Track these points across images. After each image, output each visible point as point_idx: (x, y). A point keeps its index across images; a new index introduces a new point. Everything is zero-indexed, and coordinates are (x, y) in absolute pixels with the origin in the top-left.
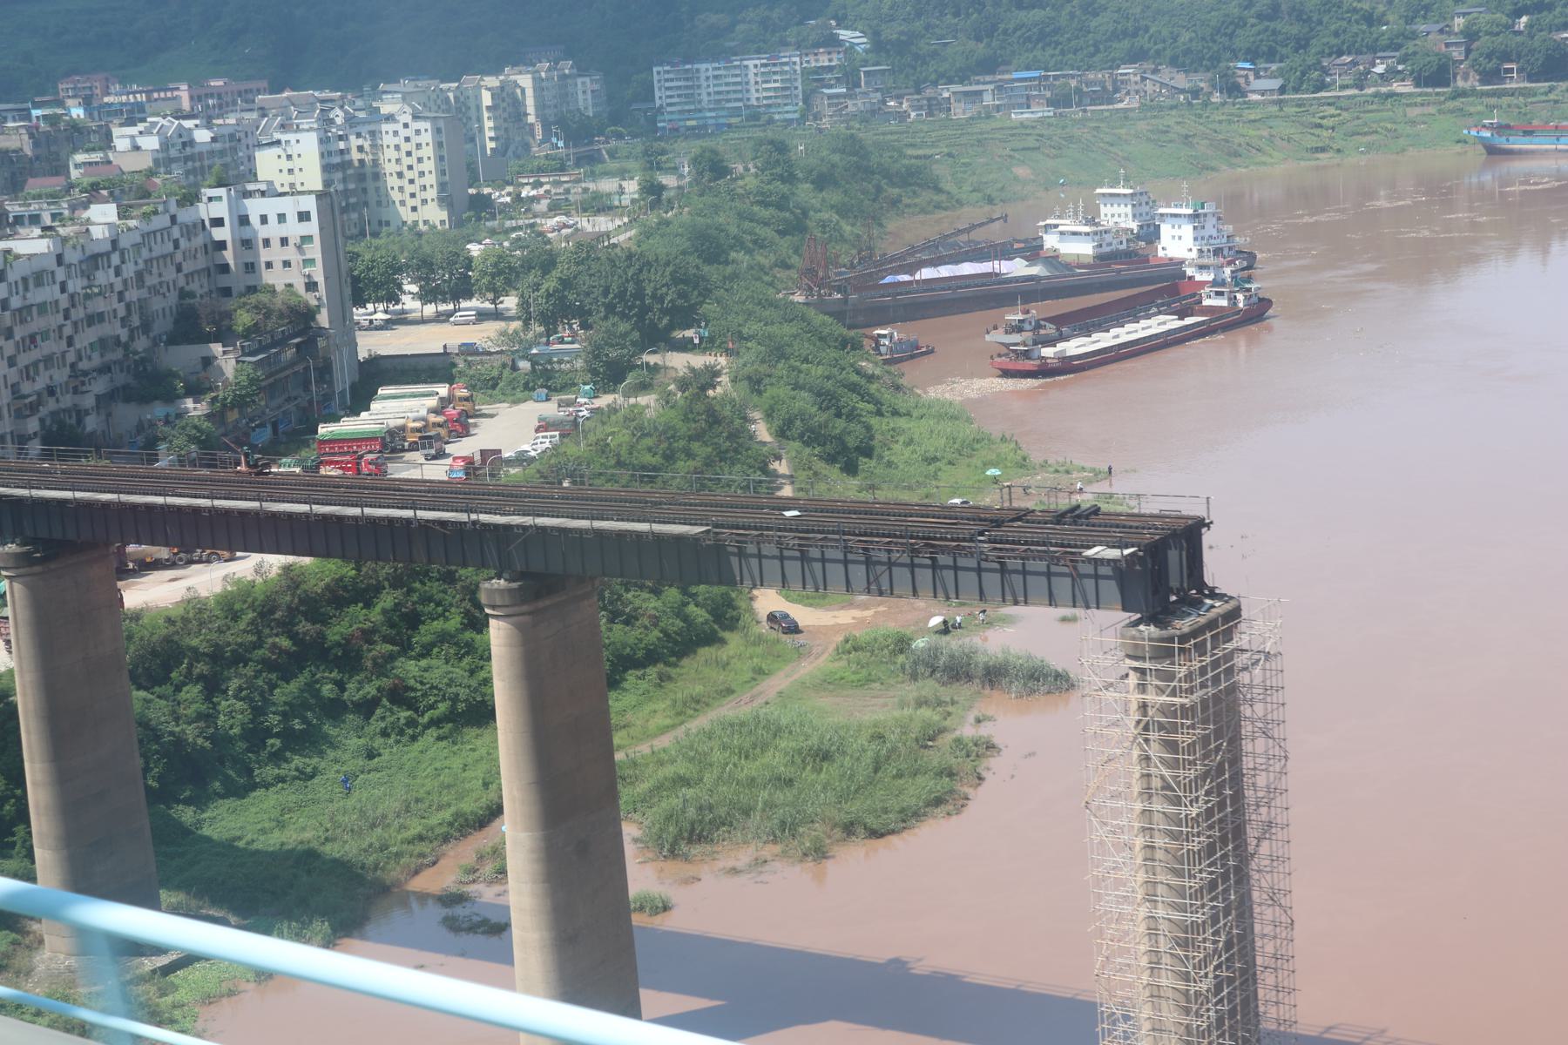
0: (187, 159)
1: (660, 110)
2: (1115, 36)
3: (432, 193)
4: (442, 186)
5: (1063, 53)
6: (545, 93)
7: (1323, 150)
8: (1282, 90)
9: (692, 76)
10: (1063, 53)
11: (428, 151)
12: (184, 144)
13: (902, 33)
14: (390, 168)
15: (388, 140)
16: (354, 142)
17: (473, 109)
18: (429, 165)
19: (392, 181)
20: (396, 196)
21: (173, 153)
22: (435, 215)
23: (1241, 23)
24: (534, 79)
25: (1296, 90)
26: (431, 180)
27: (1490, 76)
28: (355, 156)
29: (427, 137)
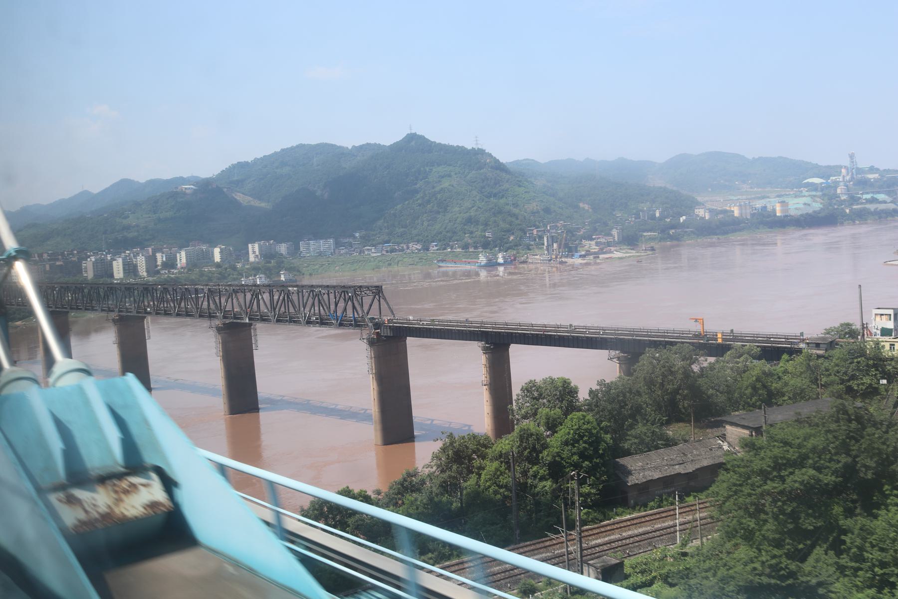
0: (102, 263)
1: (301, 252)
2: (416, 235)
3: (144, 270)
4: (147, 269)
5: (404, 239)
6: (262, 248)
7: (412, 264)
8: (437, 250)
9: (309, 244)
10: (404, 239)
11: (144, 262)
12: (102, 260)
13: (364, 234)
14: (139, 265)
15: (138, 260)
16: (134, 260)
17: (211, 252)
18: (144, 265)
19: (139, 267)
20: (139, 270)
21: (98, 261)
22: (145, 274)
23: (441, 233)
24: (259, 245)
25: (440, 250)
26: (144, 267)
27: (476, 248)
28: (134, 262)
29: (144, 259)
